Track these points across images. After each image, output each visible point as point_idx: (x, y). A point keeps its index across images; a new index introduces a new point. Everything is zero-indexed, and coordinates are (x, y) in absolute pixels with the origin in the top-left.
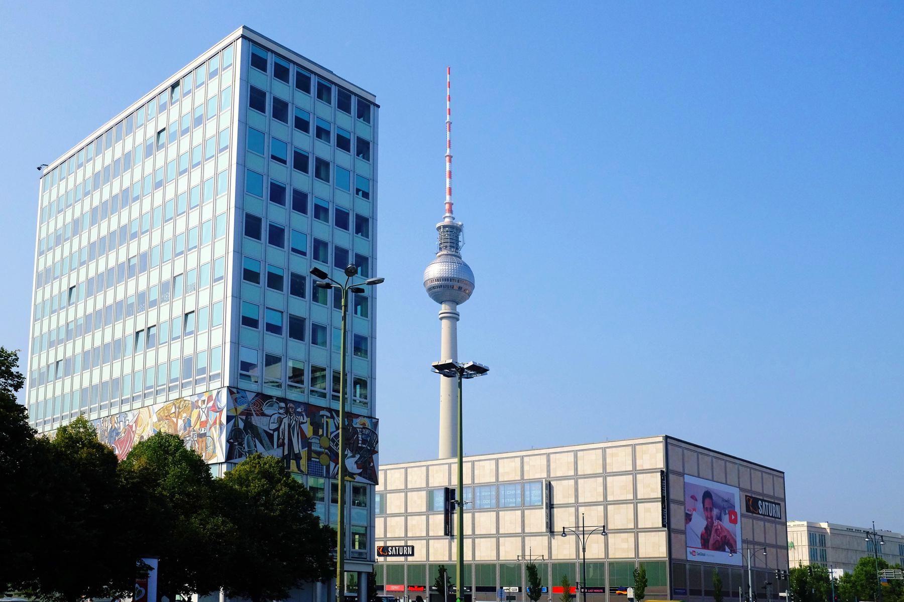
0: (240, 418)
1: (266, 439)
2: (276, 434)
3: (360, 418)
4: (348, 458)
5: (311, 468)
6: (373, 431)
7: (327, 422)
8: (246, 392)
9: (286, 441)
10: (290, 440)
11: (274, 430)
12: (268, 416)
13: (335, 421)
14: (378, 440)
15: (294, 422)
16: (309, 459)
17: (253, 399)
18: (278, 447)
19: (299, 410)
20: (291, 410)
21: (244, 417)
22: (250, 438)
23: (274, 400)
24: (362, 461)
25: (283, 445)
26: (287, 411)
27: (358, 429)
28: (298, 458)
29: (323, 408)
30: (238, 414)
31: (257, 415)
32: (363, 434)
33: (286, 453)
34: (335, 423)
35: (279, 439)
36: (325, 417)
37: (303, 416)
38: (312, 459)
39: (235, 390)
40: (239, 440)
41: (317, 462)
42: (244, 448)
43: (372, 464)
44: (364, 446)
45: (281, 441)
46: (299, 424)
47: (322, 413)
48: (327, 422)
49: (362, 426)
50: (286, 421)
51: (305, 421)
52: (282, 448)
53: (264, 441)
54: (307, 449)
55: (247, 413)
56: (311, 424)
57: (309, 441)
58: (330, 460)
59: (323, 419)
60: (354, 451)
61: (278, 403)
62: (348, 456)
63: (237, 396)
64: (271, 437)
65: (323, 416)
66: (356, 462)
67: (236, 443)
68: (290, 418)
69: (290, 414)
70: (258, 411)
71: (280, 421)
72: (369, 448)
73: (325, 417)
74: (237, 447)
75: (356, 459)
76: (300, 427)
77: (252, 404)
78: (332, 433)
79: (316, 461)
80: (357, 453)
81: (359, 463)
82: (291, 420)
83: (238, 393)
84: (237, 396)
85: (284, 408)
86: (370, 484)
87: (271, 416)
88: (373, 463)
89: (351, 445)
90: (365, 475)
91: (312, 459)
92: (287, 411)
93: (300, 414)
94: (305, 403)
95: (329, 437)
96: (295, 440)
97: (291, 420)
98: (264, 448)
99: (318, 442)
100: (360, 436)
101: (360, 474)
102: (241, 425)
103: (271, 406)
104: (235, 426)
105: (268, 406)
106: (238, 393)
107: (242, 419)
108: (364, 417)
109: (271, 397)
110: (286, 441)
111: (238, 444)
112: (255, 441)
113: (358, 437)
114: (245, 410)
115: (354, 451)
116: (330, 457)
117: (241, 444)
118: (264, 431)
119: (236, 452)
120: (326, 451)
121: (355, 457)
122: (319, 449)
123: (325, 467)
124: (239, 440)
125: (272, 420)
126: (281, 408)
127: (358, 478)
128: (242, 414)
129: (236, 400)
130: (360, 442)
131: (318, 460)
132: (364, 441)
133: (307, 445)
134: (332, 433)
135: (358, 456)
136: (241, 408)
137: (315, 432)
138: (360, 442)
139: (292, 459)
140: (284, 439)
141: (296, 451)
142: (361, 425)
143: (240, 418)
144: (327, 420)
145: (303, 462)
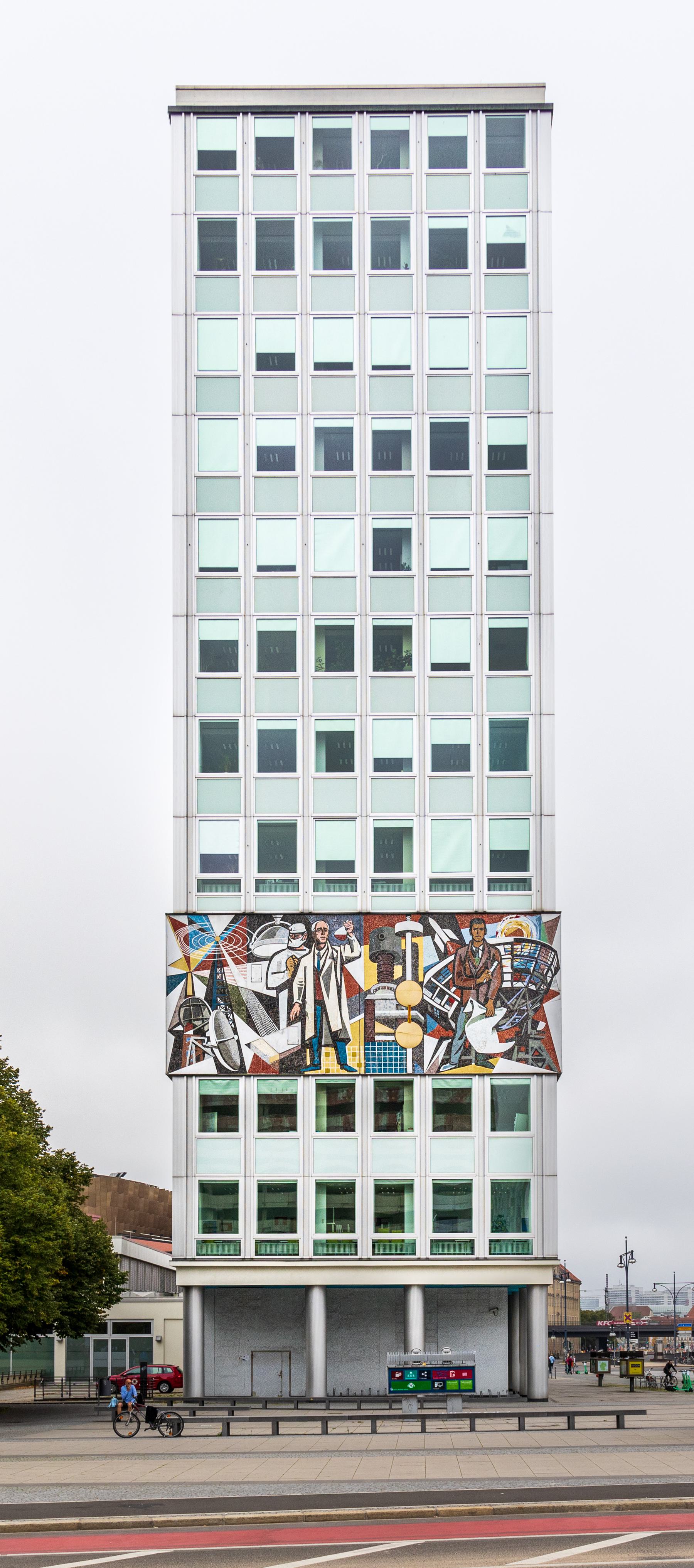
0: (195, 975)
1: (259, 1011)
2: (284, 996)
4: (469, 1024)
5: (374, 1059)
6: (543, 945)
7: (415, 947)
8: (210, 917)
9: (310, 1009)
10: (320, 1003)
11: (279, 989)
12: (263, 959)
13: (437, 940)
14: (558, 964)
15: (329, 962)
16: (369, 1039)
17: (226, 929)
18: (290, 1023)
19: (341, 931)
20: (319, 935)
21: (206, 973)
22: (222, 1015)
23: (278, 921)
24: (513, 1024)
25: (302, 1017)
26: (311, 941)
27: (501, 948)
28: (339, 1041)
29: (403, 916)
30: (192, 968)
31: (237, 962)
32: (514, 957)
33: (310, 1033)
34: (435, 944)
35: (290, 1006)
36: (409, 935)
37: (350, 942)
38: (377, 1038)
39: (184, 920)
40: (196, 1023)
41: (390, 1043)
42: (209, 1040)
43: (541, 1026)
44: (520, 985)
45: (296, 1009)
46: (342, 964)
47: (399, 927)
48: (415, 947)
49: (511, 939)
50: (308, 963)
51: (356, 954)
52: (299, 1024)
53: (254, 1017)
54: (362, 1016)
55: (216, 963)
56: (373, 958)
57: (369, 997)
58: (425, 1032)
59: (403, 941)
60: (490, 1002)
61: (286, 927)
62: (473, 1016)
63: (189, 929)
64: (270, 1005)
65: (402, 934)
66: (497, 1027)
68: (319, 954)
69: (318, 943)
70: (238, 953)
71: (295, 965)
72: (533, 987)
73: (409, 935)
74: (192, 1039)
75: (494, 1020)
76: (343, 969)
77: (225, 940)
78: (427, 969)
80: (499, 1003)
81: (504, 1027)
82: (320, 958)
83: (191, 922)
84: (189, 929)
85: (303, 934)
87: (270, 959)
88: (546, 1021)
89: (483, 989)
91: (377, 1038)
92: (311, 941)
93: (344, 940)
95: (421, 980)
96: (331, 1002)
97: (320, 958)
98: (257, 1031)
99: (391, 995)
100: (507, 963)
101: (508, 1055)
102: (200, 991)
103: (272, 935)
104: (186, 996)
105: (264, 938)
106: (191, 922)
107: (201, 979)
108: (518, 914)
109: (269, 917)
110: (310, 1009)
112: (234, 1022)
113: (501, 966)
114: (209, 956)
115: (490, 1002)
116: (424, 1027)
117: (201, 1032)
118: (256, 993)
119: (191, 1052)
120: (414, 1013)
121: (493, 1015)
122: (395, 1013)
123: (409, 1052)
124: (196, 1023)
125: (274, 967)
126: (295, 936)
127: (502, 1065)
128: (201, 966)
129: (186, 940)
130: (507, 977)
131: (391, 1038)
132: (517, 974)
133: (362, 1007)
134: (427, 969)
135: (501, 1012)
136: (198, 955)
137: (385, 976)
138: (507, 977)
139: (325, 1046)
140: (303, 1006)
141: (336, 1026)
142: (510, 935)
143: (195, 975)
144: (415, 940)
145: (355, 1052)
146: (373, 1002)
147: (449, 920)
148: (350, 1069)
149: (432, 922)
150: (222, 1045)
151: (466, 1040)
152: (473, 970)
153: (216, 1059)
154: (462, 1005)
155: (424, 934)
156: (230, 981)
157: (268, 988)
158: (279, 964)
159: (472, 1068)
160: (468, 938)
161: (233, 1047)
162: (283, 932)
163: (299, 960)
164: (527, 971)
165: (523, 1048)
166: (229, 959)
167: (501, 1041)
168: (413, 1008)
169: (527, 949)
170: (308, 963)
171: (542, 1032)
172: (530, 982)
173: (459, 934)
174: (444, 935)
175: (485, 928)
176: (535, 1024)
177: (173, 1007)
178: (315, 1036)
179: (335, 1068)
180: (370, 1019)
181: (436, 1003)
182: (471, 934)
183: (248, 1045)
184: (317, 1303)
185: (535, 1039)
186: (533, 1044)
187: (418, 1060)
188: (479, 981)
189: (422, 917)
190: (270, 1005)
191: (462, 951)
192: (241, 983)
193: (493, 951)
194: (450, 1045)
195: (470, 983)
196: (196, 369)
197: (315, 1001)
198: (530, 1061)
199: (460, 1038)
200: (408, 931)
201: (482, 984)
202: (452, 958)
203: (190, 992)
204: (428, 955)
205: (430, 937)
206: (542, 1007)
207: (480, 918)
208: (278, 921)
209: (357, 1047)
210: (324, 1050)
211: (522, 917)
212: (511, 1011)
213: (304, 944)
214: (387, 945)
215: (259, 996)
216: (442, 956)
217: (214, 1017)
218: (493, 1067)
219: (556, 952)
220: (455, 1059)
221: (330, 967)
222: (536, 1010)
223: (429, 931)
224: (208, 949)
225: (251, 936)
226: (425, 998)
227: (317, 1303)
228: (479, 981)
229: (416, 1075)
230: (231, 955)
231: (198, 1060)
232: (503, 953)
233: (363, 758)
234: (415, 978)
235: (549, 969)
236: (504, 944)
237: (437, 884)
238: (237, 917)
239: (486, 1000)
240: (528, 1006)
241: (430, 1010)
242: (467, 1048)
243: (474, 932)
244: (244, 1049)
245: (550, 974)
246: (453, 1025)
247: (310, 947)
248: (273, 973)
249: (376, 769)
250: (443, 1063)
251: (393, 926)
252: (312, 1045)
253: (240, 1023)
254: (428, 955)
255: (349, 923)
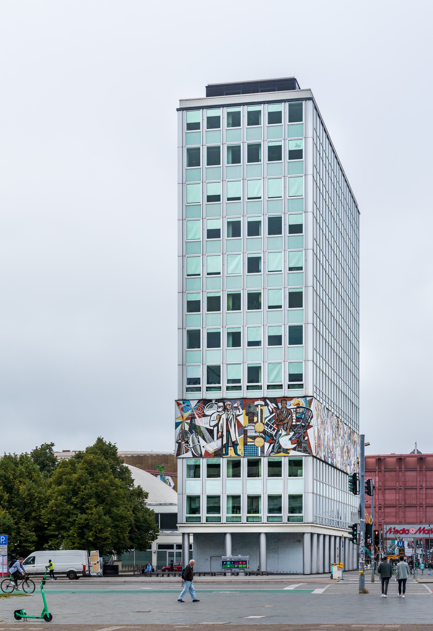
1: (207, 435)
2: (216, 429)
3: (294, 400)
4: (281, 437)
5: (247, 451)
6: (307, 409)
7: (261, 410)
8: (190, 401)
9: (225, 433)
10: (228, 431)
11: (214, 426)
12: (209, 416)
13: (269, 407)
14: (312, 415)
15: (231, 416)
16: (245, 444)
17: (196, 405)
18: (218, 439)
19: (236, 405)
20: (228, 407)
21: (189, 421)
22: (194, 436)
23: (214, 402)
24: (296, 437)
25: (222, 437)
26: (225, 409)
27: (292, 410)
28: (235, 445)
29: (257, 399)
30: (184, 420)
31: (199, 417)
32: (297, 413)
33: (225, 442)
34: (269, 409)
35: (218, 432)
37: (239, 409)
38: (248, 443)
39: (181, 402)
40: (185, 439)
41: (253, 445)
42: (190, 445)
43: (306, 438)
44: (299, 423)
45: (220, 433)
46: (236, 417)
48: (261, 410)
49: (296, 407)
50: (224, 417)
51: (241, 413)
52: (221, 439)
53: (205, 437)
54: (243, 435)
55: (192, 418)
56: (247, 414)
57: (245, 429)
58: (265, 441)
59: (257, 408)
60: (288, 430)
61: (217, 404)
63: (183, 405)
65: (257, 406)
66: (290, 439)
67: (184, 442)
68: (228, 413)
69: (228, 409)
70: (200, 414)
71: (220, 417)
72: (303, 424)
73: (259, 406)
74: (184, 445)
76: (236, 419)
77: (195, 409)
78: (266, 418)
79: (251, 445)
80: (291, 430)
81: (293, 439)
82: (228, 415)
83: (184, 403)
84: (183, 405)
85: (222, 406)
86: (305, 456)
87: (211, 416)
88: (308, 436)
89: (285, 425)
90: (299, 449)
91: (248, 443)
92: (225, 409)
93: (236, 408)
94: (242, 398)
96: (232, 431)
97: (228, 415)
98: (206, 442)
99: (253, 428)
100: (294, 415)
101: (294, 449)
102: (187, 428)
103: (211, 407)
105: (209, 408)
106: (184, 403)
107: (187, 423)
108: (298, 397)
109: (210, 401)
110: (225, 433)
111: (185, 443)
112: (198, 438)
113: (292, 417)
114: (190, 415)
115: (288, 430)
117: (187, 442)
118: (206, 428)
119: (183, 449)
120: (261, 434)
121: (289, 434)
122: (254, 434)
123: (259, 448)
124: (185, 439)
125: (212, 419)
126: (219, 407)
127: (292, 453)
128: (187, 419)
129: (182, 409)
130: (294, 421)
131: (253, 443)
132: (298, 419)
133: (243, 432)
134: (266, 418)
135: (292, 434)
136: (186, 415)
137: (251, 421)
138: (294, 421)
139: (230, 447)
140: (222, 432)
141: (234, 439)
142: (295, 405)
144: (262, 408)
145: (240, 448)
146: (247, 430)
147: (274, 400)
148: (239, 455)
149: (268, 401)
150: (194, 447)
151: (280, 443)
152: (282, 418)
153: (192, 452)
154: (278, 431)
155: (265, 406)
156: (197, 424)
157: (210, 426)
158: (214, 417)
159: (282, 454)
160: (280, 407)
161: (198, 447)
162: (215, 405)
163: (221, 416)
164: (301, 418)
165: (300, 447)
166: (197, 416)
167: (292, 444)
168: (261, 433)
169: (301, 410)
170: (224, 417)
171: (307, 440)
172: (302, 422)
173: (277, 405)
174: (272, 406)
175: (286, 403)
176: (304, 438)
177: (178, 434)
178: (226, 443)
179: (233, 455)
180: (246, 437)
181: (269, 430)
182: (281, 405)
183: (203, 447)
184: (228, 539)
185: (304, 443)
186: (303, 445)
187: (262, 451)
188: (284, 422)
189: (264, 399)
190: (211, 432)
191: (278, 411)
192: (201, 424)
193: (289, 411)
194: (274, 446)
195: (280, 423)
196: (186, 203)
197: (226, 430)
198: (302, 451)
199: (278, 443)
200: (259, 405)
201: (285, 423)
202: (274, 414)
203: (183, 428)
204: (266, 413)
205: (267, 406)
206: (306, 431)
207: (285, 399)
208: (214, 402)
209: (241, 447)
210: (229, 448)
211: (300, 399)
212: (295, 433)
213: (223, 410)
214: (252, 410)
215: (207, 429)
216: (271, 413)
217: (191, 437)
218: (289, 453)
219: (311, 411)
220: (275, 450)
221: (232, 418)
222: (304, 433)
223: (266, 404)
224: (190, 412)
225: (204, 407)
226: (265, 429)
227: (228, 539)
228: (284, 422)
229: (262, 457)
230: (197, 414)
231: (186, 452)
232: (293, 412)
233: (244, 341)
234: (262, 421)
235: (309, 417)
236: (293, 409)
237: (269, 387)
238: (200, 401)
239: (287, 429)
240: (302, 431)
241: (267, 433)
242: (280, 447)
243: (283, 404)
244: (202, 448)
245: (309, 419)
246: (275, 438)
247: (225, 411)
248: (212, 421)
249: (248, 346)
250: (272, 452)
251: (254, 403)
252: (225, 447)
253: (201, 439)
254: (266, 413)
255: (238, 402)
